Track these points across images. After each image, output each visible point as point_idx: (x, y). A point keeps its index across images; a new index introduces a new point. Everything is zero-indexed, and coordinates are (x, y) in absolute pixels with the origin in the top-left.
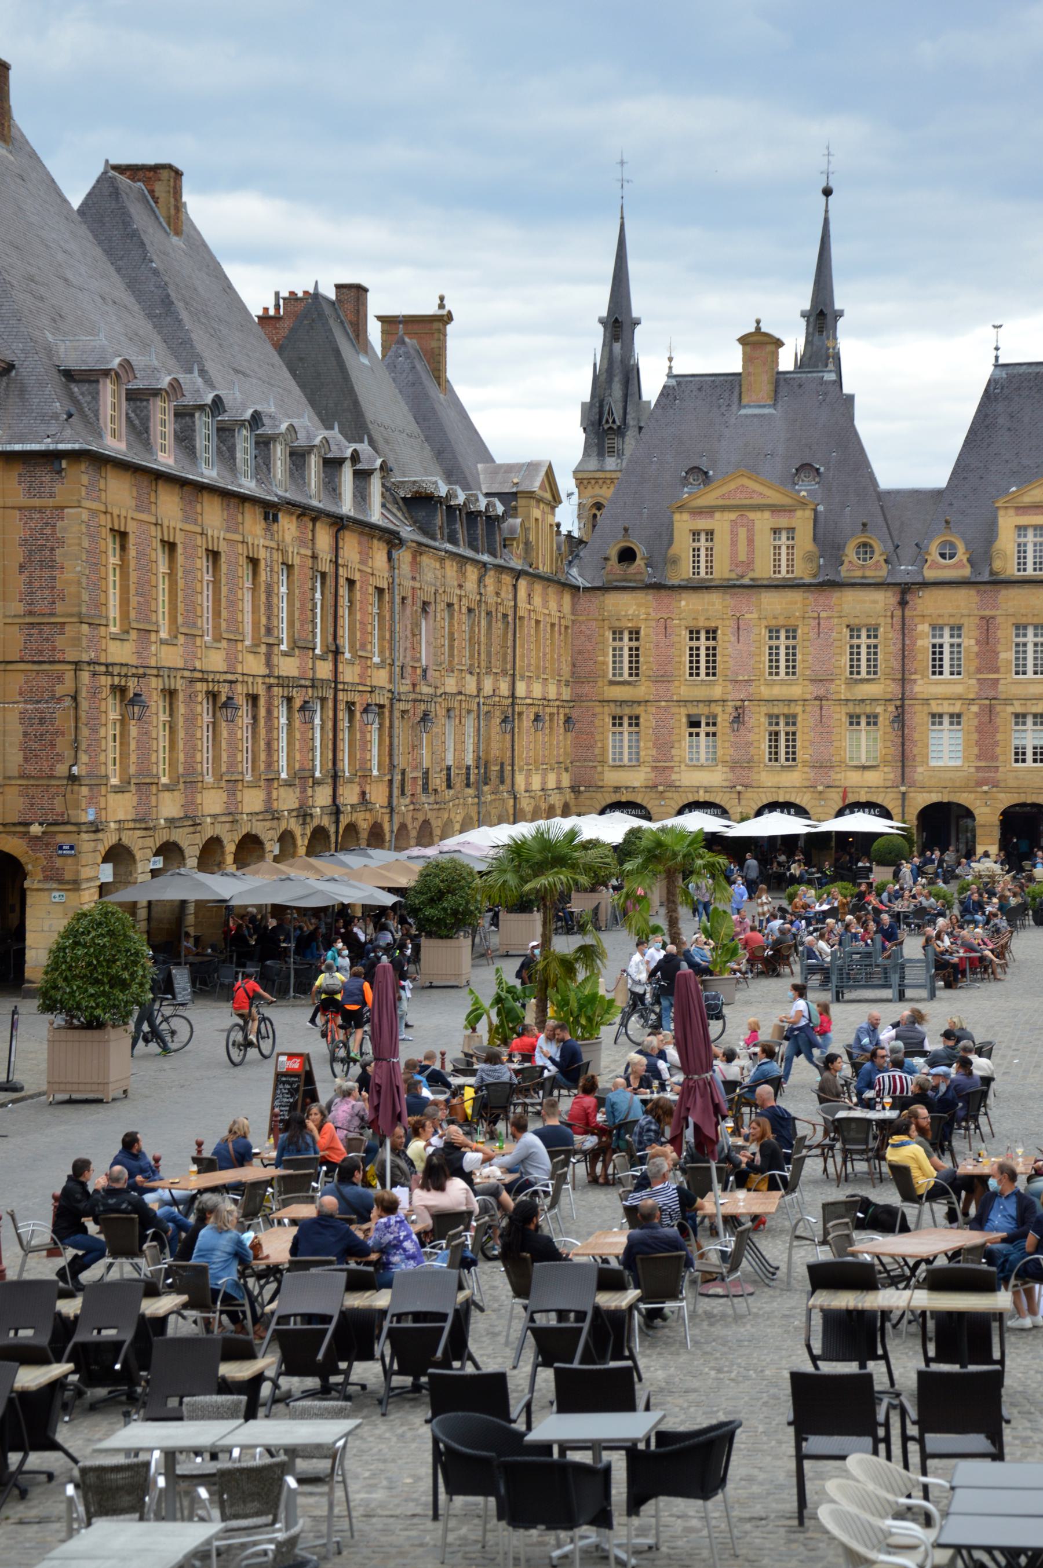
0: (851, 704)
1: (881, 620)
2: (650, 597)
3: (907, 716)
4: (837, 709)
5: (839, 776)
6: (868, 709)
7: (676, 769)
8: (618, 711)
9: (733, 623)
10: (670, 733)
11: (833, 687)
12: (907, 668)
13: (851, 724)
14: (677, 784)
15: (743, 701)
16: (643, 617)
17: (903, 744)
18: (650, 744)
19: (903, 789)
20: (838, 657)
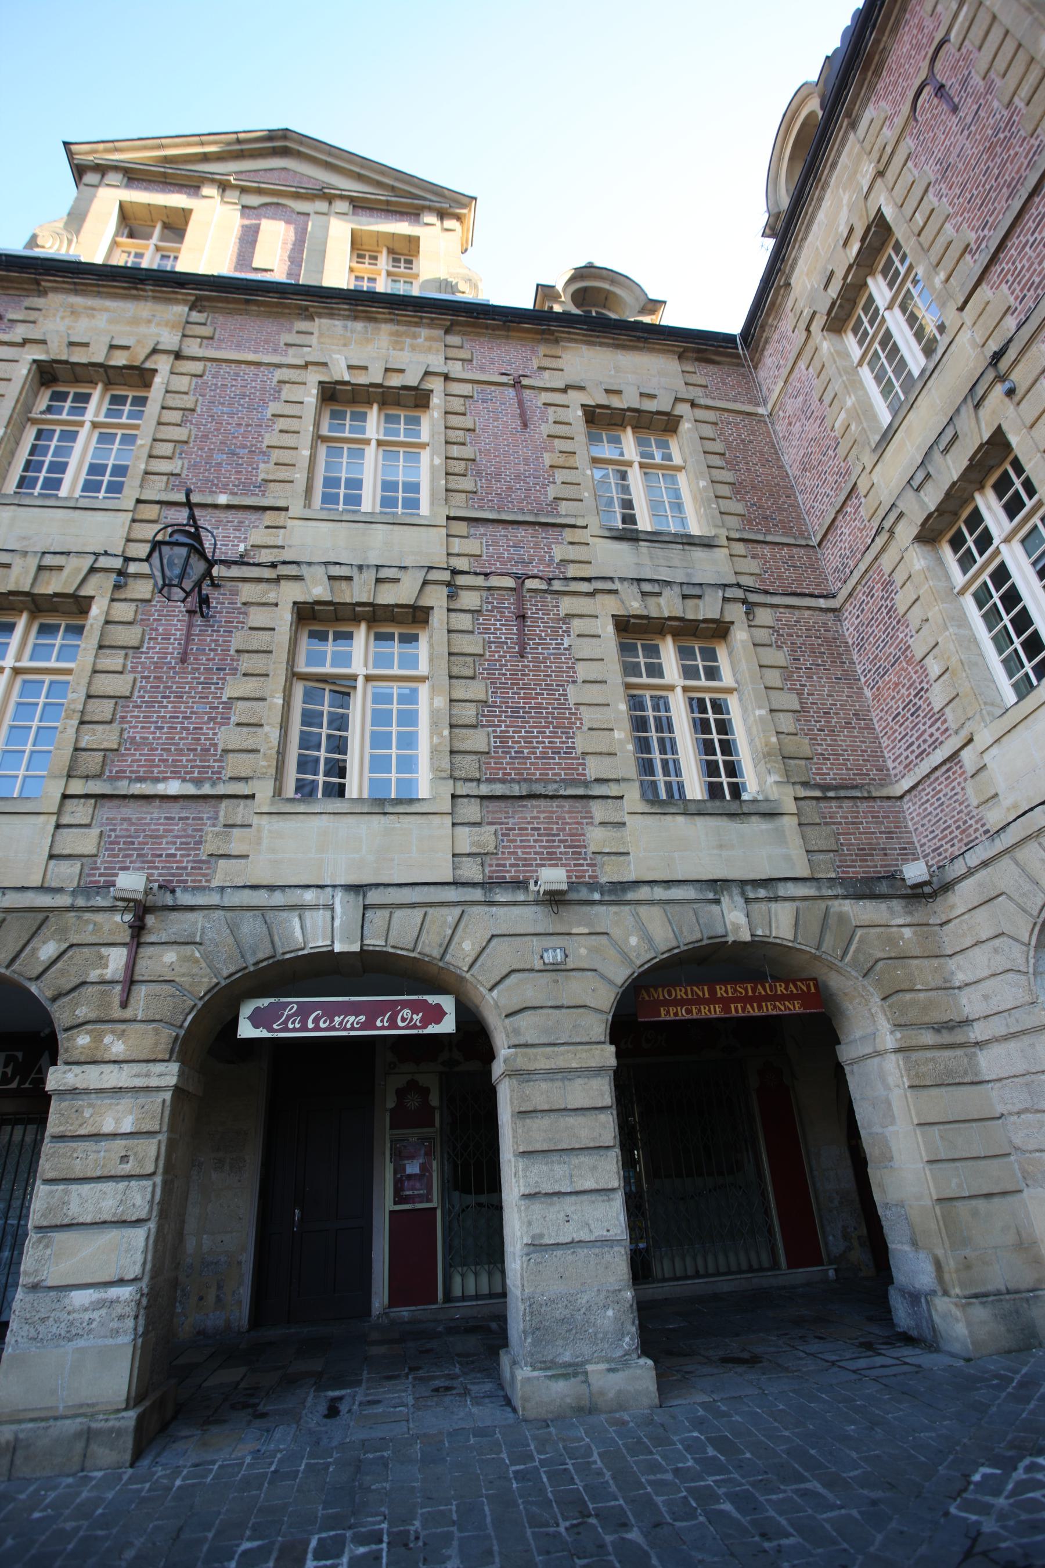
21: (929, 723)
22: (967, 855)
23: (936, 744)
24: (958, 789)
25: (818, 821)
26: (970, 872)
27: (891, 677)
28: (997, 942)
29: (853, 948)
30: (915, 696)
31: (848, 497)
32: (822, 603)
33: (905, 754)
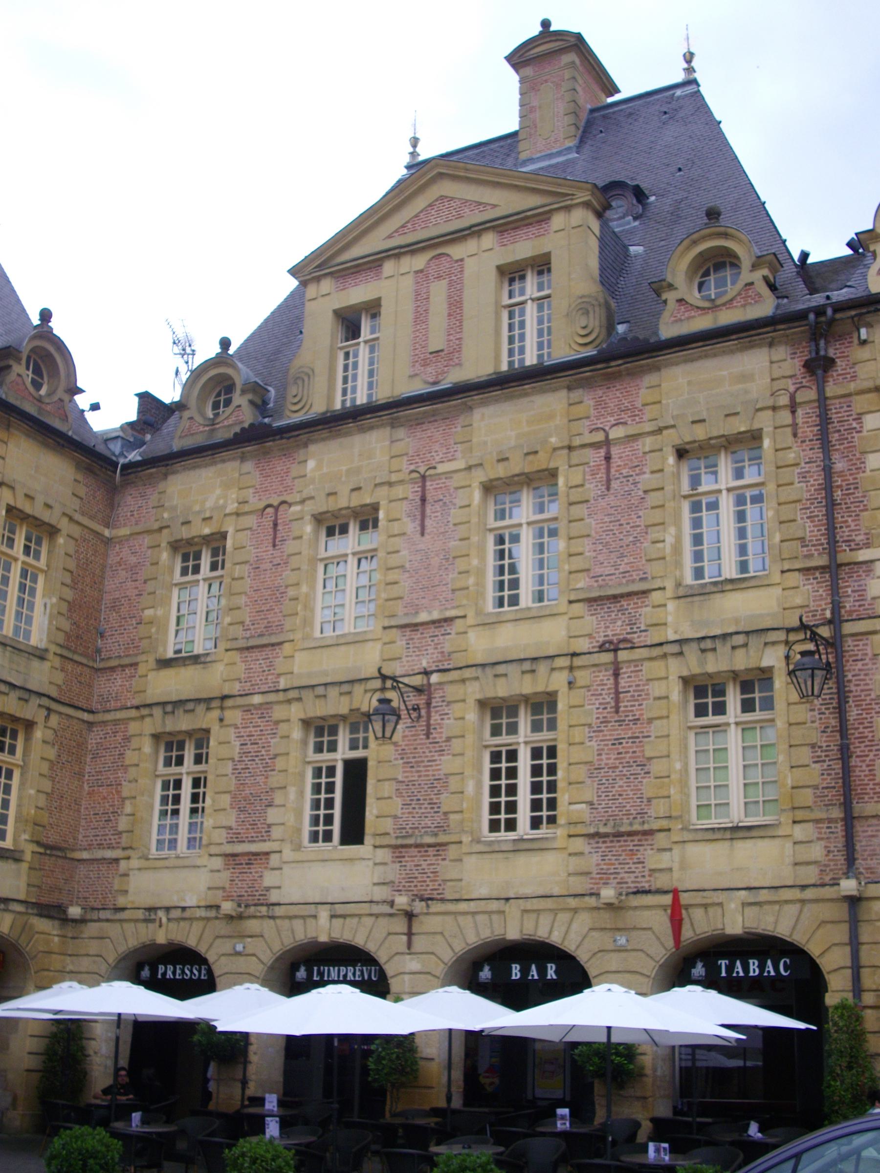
0: (692, 653)
1: (765, 421)
2: (248, 466)
3: (852, 670)
4: (656, 668)
5: (665, 860)
6: (741, 661)
7: (274, 860)
8: (171, 725)
9: (411, 491)
10: (269, 768)
11: (646, 613)
12: (843, 534)
13: (701, 711)
14: (274, 897)
15: (427, 673)
16: (232, 507)
17: (845, 753)
18: (226, 800)
19: (849, 886)
20: (654, 534)
21: (112, 832)
22: (101, 912)
23: (110, 847)
24: (110, 876)
25: (37, 867)
26: (99, 920)
27: (104, 791)
28: (96, 959)
29: (31, 943)
30: (112, 813)
31: (131, 665)
32: (86, 716)
33: (92, 838)
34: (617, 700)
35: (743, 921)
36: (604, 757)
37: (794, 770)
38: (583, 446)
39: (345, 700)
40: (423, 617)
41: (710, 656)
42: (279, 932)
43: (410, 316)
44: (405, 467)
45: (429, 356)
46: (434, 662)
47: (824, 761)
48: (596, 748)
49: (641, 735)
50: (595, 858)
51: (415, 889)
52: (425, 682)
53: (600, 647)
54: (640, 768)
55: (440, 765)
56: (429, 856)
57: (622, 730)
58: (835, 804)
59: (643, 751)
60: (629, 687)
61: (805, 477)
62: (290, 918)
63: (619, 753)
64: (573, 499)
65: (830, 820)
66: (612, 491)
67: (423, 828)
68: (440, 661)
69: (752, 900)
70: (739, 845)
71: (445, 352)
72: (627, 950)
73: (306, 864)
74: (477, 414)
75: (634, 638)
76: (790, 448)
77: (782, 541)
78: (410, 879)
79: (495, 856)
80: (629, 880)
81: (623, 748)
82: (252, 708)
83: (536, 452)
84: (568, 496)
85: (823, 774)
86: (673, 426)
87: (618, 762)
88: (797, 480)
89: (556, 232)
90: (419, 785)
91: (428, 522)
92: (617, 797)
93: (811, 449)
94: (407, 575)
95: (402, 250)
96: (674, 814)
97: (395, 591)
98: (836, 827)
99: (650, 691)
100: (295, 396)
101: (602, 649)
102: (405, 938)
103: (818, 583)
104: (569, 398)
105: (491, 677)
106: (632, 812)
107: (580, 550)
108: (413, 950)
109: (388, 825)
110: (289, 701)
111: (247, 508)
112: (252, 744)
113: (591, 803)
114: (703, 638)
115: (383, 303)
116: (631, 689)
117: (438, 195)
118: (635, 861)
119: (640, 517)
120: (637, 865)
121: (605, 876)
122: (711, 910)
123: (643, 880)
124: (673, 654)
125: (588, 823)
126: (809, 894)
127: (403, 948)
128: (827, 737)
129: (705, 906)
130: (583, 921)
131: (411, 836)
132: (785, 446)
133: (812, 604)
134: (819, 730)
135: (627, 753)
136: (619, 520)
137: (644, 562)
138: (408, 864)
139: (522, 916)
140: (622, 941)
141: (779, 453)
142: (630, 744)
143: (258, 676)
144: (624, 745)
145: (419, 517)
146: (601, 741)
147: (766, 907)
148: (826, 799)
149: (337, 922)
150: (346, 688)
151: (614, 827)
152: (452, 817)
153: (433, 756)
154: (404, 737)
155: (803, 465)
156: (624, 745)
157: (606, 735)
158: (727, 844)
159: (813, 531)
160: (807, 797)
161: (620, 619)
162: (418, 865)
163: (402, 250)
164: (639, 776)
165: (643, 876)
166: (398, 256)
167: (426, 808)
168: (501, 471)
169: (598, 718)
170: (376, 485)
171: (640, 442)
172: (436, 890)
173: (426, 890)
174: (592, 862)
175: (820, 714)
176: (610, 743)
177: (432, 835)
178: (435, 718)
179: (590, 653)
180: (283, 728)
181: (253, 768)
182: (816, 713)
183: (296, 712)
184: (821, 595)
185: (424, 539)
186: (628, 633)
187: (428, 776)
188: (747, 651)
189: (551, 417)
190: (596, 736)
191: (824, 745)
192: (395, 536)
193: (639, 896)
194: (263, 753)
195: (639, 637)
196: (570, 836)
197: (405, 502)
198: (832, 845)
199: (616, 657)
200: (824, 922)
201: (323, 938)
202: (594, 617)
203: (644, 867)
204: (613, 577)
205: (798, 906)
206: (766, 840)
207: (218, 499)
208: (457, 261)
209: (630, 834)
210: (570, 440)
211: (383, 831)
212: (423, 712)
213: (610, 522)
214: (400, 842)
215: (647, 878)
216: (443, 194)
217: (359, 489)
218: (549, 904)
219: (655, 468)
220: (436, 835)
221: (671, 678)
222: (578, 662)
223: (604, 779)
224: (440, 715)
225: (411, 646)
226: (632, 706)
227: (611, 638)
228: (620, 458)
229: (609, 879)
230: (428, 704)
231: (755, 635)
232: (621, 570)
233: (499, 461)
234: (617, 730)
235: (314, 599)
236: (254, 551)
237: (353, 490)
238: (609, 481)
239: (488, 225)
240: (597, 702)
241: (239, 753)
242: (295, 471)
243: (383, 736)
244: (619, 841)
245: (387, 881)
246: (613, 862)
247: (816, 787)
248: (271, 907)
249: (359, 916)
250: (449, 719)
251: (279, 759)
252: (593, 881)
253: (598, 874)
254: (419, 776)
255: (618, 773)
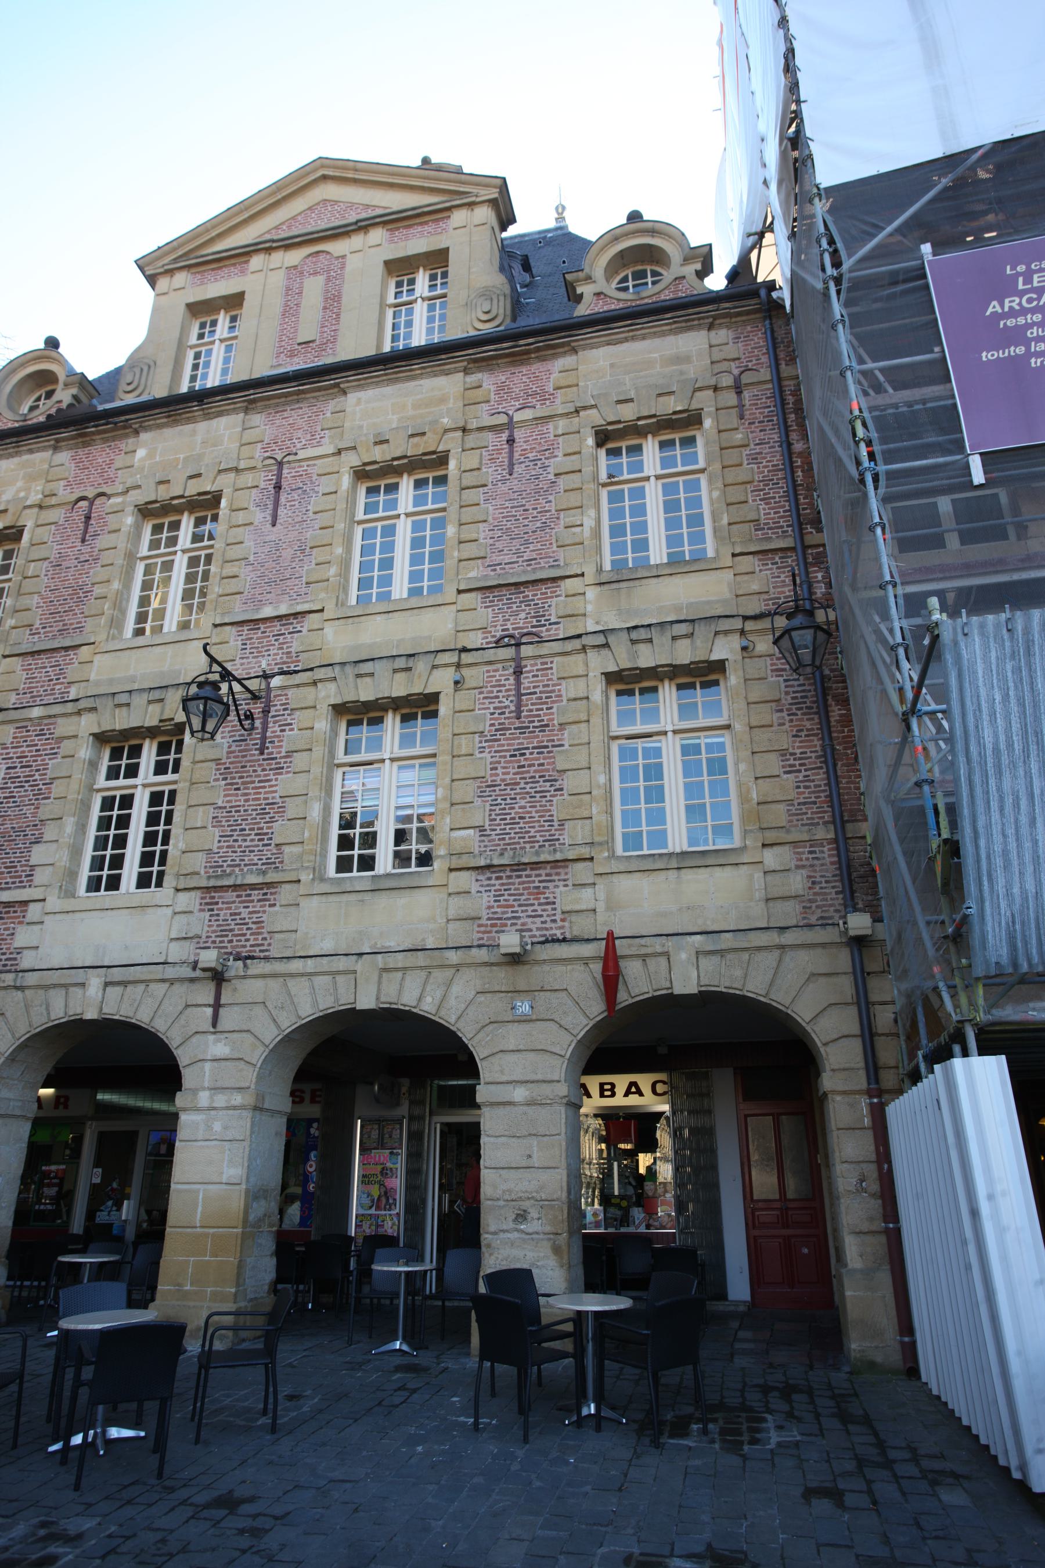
1: (705, 401)
2: (64, 457)
5: (585, 898)
7: (34, 911)
9: (264, 479)
11: (556, 605)
14: (27, 961)
15: (266, 676)
34: (519, 706)
35: (699, 976)
36: (500, 771)
37: (760, 781)
38: (480, 429)
39: (154, 708)
40: (268, 612)
41: (642, 647)
42: (27, 1007)
43: (278, 309)
44: (258, 454)
45: (297, 347)
46: (276, 664)
47: (800, 771)
48: (489, 760)
49: (550, 744)
50: (486, 899)
51: (229, 945)
52: (263, 686)
53: (497, 642)
54: (548, 784)
55: (276, 785)
56: (253, 901)
57: (524, 738)
58: (818, 824)
59: (554, 763)
60: (534, 687)
61: (756, 459)
62: (46, 987)
63: (519, 767)
64: (465, 483)
65: (813, 843)
66: (515, 475)
67: (245, 865)
68: (284, 663)
69: (711, 948)
70: (688, 875)
71: (318, 343)
72: (531, 1021)
73: (78, 915)
74: (352, 397)
75: (542, 632)
76: (737, 429)
77: (730, 524)
78: (224, 932)
79: (345, 898)
80: (533, 927)
81: (526, 759)
82: (29, 723)
83: (424, 434)
84: (460, 479)
85: (798, 787)
86: (592, 407)
87: (518, 776)
88: (746, 462)
89: (455, 229)
90: (245, 811)
91: (281, 512)
92: (517, 820)
93: (761, 431)
94: (250, 568)
95: (274, 245)
96: (597, 839)
97: (232, 586)
98: (823, 852)
99: (563, 692)
100: (129, 384)
101: (499, 643)
102: (209, 1011)
103: (778, 568)
104: (465, 383)
105: (351, 678)
106: (538, 838)
107: (474, 536)
108: (219, 1028)
109: (198, 862)
110: (79, 713)
111: (53, 501)
112: (22, 767)
113: (481, 829)
114: (635, 627)
115: (246, 296)
116: (537, 690)
117: (320, 198)
118: (542, 901)
119: (550, 502)
120: (543, 907)
121: (498, 922)
122: (651, 962)
123: (553, 925)
124: (594, 647)
125: (476, 852)
126: (788, 938)
127: (207, 1026)
128: (801, 742)
129: (644, 957)
130: (463, 988)
131: (230, 875)
132: (729, 427)
133: (772, 590)
134: (790, 734)
135: (530, 766)
136: (524, 505)
137: (555, 548)
138: (222, 913)
139: (380, 977)
140: (524, 1007)
141: (722, 434)
142: (535, 755)
143: (42, 686)
144: (528, 756)
145: (271, 507)
146: (496, 752)
147: (729, 956)
148: (805, 817)
149: (114, 992)
150: (156, 695)
151: (514, 857)
152: (287, 849)
153: (268, 775)
154: (229, 753)
155: (752, 446)
156: (528, 756)
157: (503, 745)
158: (672, 875)
159: (769, 514)
160: (779, 814)
161: (524, 610)
162: (235, 914)
163: (274, 245)
164: (548, 794)
165: (554, 921)
166: (269, 250)
167: (252, 840)
168: (379, 454)
169: (492, 725)
170: (220, 471)
171: (551, 426)
172: (259, 945)
173: (244, 946)
174: (482, 903)
175: (789, 715)
176: (508, 754)
177: (258, 874)
178: (273, 728)
179: (484, 649)
180: (67, 746)
181: (20, 797)
182: (785, 714)
183: (88, 724)
184: (784, 581)
185: (275, 529)
186: (533, 627)
187: (259, 799)
188: (692, 643)
189: (443, 400)
190: (489, 747)
191: (798, 751)
192: (239, 526)
193: (548, 945)
194: (37, 777)
195: (547, 630)
196: (451, 870)
197: (254, 491)
198: (818, 874)
199: (518, 652)
200: (813, 975)
201: (91, 1015)
202: (490, 610)
203: (555, 909)
204: (516, 565)
205: (777, 953)
206: (728, 869)
207: (18, 491)
208: (338, 258)
209: (536, 865)
210: (466, 422)
211: (190, 870)
212: (258, 723)
213: (512, 507)
214: (212, 883)
215: (560, 924)
216: (325, 197)
217: (199, 475)
218: (421, 959)
219: (570, 451)
220: (264, 873)
221: (591, 674)
222: (466, 658)
223: (499, 798)
224: (280, 726)
225: (248, 646)
226: (537, 710)
227: (511, 632)
228: (525, 442)
229: (506, 925)
230: (266, 712)
231: (703, 623)
232: (525, 558)
233: (376, 443)
234: (519, 738)
235: (128, 601)
236: (56, 547)
237: (191, 477)
238: (511, 465)
239: (378, 220)
240: (492, 706)
241: (4, 779)
242: (120, 461)
243: (203, 730)
244: (520, 876)
245: (190, 935)
246: (511, 903)
247: (790, 802)
248: (21, 974)
249: (146, 982)
250: (292, 730)
251: (57, 782)
252: (482, 929)
253: (489, 919)
254: (247, 801)
255: (518, 791)
